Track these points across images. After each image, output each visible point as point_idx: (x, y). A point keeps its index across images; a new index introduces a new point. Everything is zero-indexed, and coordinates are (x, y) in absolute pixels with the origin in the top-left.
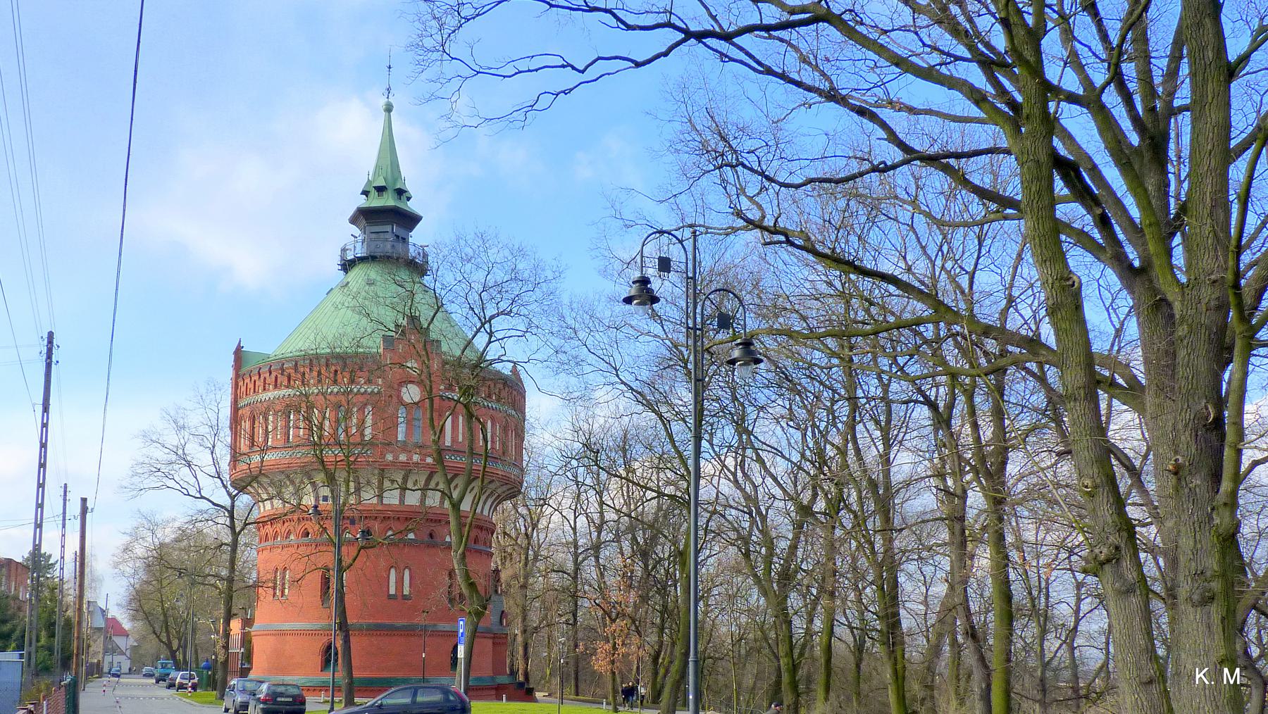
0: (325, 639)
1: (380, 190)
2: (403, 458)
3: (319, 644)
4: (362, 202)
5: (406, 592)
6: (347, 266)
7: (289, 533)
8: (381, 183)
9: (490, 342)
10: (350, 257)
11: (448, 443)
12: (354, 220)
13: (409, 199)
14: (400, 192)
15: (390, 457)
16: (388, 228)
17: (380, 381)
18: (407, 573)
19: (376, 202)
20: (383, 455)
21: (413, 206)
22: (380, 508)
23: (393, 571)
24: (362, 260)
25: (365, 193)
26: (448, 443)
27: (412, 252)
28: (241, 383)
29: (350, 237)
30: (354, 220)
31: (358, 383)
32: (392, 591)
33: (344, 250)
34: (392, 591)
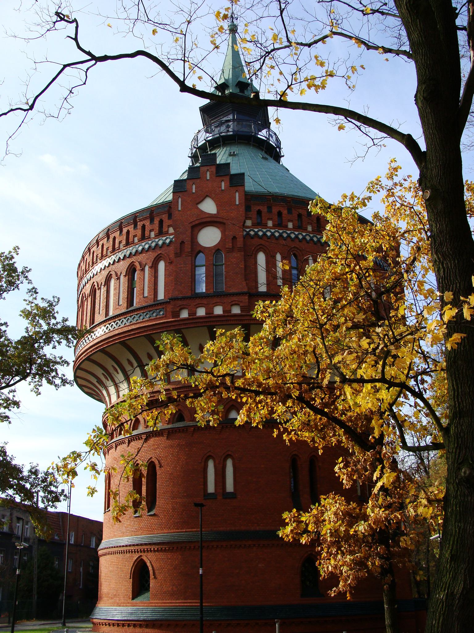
0: (136, 556)
2: (201, 312)
5: (230, 487)
14: (244, 86)
15: (185, 314)
16: (231, 117)
17: (171, 230)
18: (229, 464)
20: (176, 314)
23: (211, 465)
31: (149, 238)
32: (211, 488)
34: (211, 488)
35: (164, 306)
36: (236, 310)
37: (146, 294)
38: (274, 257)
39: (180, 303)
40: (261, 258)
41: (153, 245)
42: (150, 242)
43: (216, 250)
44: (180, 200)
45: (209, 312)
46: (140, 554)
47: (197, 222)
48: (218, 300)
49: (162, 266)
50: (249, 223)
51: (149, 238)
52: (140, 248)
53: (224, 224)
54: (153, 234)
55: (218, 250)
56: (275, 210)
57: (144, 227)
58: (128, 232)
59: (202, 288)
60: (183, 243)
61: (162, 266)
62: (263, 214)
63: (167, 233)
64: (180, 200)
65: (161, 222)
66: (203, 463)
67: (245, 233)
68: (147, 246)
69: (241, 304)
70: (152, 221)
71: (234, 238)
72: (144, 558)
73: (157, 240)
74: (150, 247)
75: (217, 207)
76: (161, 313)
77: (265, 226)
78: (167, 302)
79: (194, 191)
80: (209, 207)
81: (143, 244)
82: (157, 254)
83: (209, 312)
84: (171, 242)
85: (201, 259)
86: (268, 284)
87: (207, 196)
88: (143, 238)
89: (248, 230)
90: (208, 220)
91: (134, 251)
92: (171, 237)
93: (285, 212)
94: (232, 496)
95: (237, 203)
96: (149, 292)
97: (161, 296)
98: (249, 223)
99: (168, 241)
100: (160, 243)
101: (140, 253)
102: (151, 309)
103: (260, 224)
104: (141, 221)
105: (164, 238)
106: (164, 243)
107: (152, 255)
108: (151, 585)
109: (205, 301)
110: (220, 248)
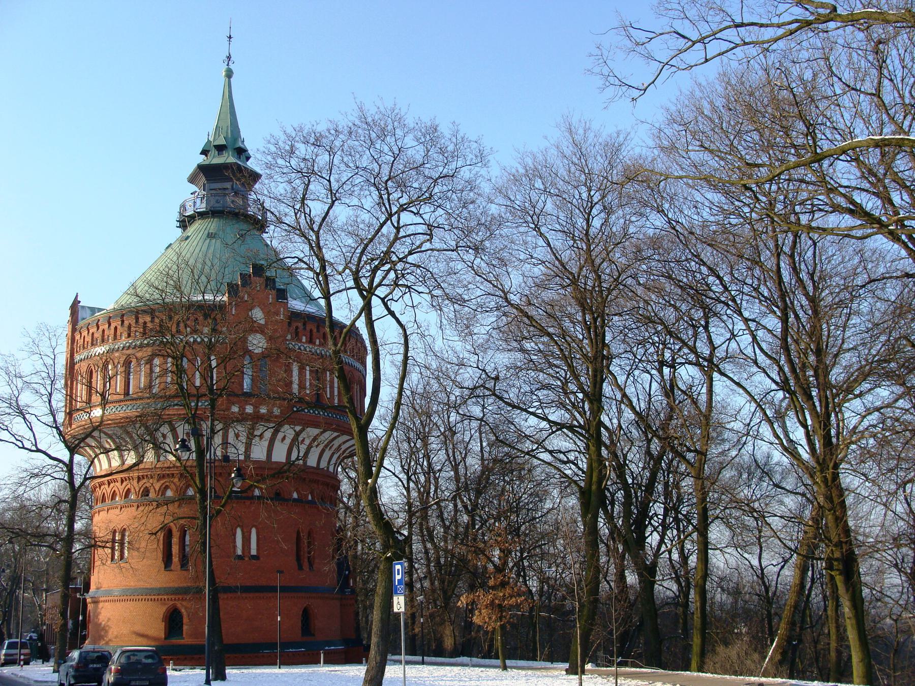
1: (220, 149)
2: (249, 409)
3: (160, 611)
4: (201, 159)
6: (185, 222)
7: (128, 491)
8: (221, 141)
9: (397, 238)
10: (189, 212)
12: (192, 180)
13: (248, 158)
14: (241, 152)
18: (254, 531)
19: (217, 159)
21: (252, 164)
23: (239, 532)
24: (202, 215)
25: (204, 152)
27: (252, 210)
28: (77, 337)
29: (187, 194)
30: (192, 180)
32: (239, 552)
33: (183, 207)
43: (264, 356)
46: (172, 603)
63: (221, 333)
72: (179, 605)
80: (258, 314)
98: (289, 337)
108: (185, 628)
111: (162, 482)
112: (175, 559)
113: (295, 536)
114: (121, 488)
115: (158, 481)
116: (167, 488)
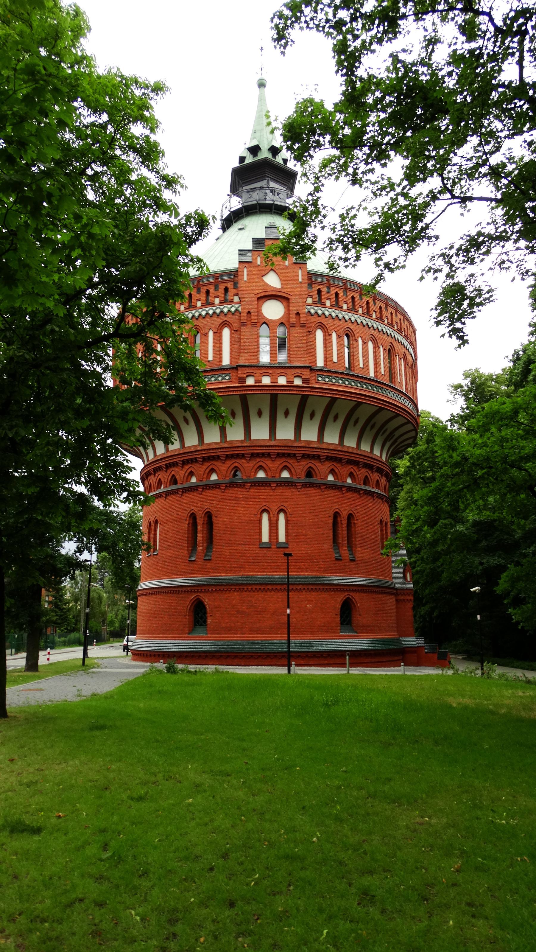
2: (266, 381)
5: (282, 538)
11: (320, 363)
15: (250, 381)
16: (263, 183)
18: (282, 517)
20: (243, 380)
22: (247, 443)
23: (265, 518)
26: (320, 363)
31: (213, 304)
32: (265, 538)
34: (265, 538)
35: (230, 372)
36: (298, 382)
37: (210, 358)
38: (330, 335)
39: (247, 370)
40: (319, 335)
41: (218, 311)
42: (214, 308)
44: (245, 270)
45: (274, 381)
47: (262, 294)
48: (282, 371)
49: (226, 333)
50: (310, 301)
51: (213, 304)
52: (204, 313)
53: (287, 299)
54: (217, 301)
55: (282, 324)
56: (333, 291)
57: (208, 292)
58: (190, 295)
59: (265, 358)
60: (249, 313)
61: (226, 333)
62: (323, 293)
63: (232, 301)
64: (245, 270)
65: (226, 290)
66: (259, 516)
67: (306, 310)
68: (211, 312)
69: (304, 377)
70: (216, 288)
71: (298, 314)
73: (222, 307)
74: (214, 313)
75: (281, 281)
76: (227, 378)
77: (324, 305)
78: (233, 368)
79: (259, 263)
80: (273, 281)
81: (207, 309)
82: (222, 321)
83: (274, 381)
84: (236, 310)
85: (264, 330)
86: (326, 360)
87: (272, 270)
88: (208, 304)
89: (309, 307)
90: (274, 293)
91: (197, 314)
92: (237, 306)
93: (341, 293)
94: (281, 546)
95: (300, 280)
96: (214, 356)
97: (226, 361)
98: (310, 301)
99: (233, 309)
100: (226, 310)
101: (204, 318)
102: (216, 373)
103: (320, 302)
104: (204, 285)
105: (229, 306)
106: (229, 311)
107: (218, 321)
109: (270, 371)
110: (284, 322)
111: (186, 467)
112: (200, 548)
113: (331, 521)
114: (154, 479)
115: (183, 466)
116: (191, 474)
